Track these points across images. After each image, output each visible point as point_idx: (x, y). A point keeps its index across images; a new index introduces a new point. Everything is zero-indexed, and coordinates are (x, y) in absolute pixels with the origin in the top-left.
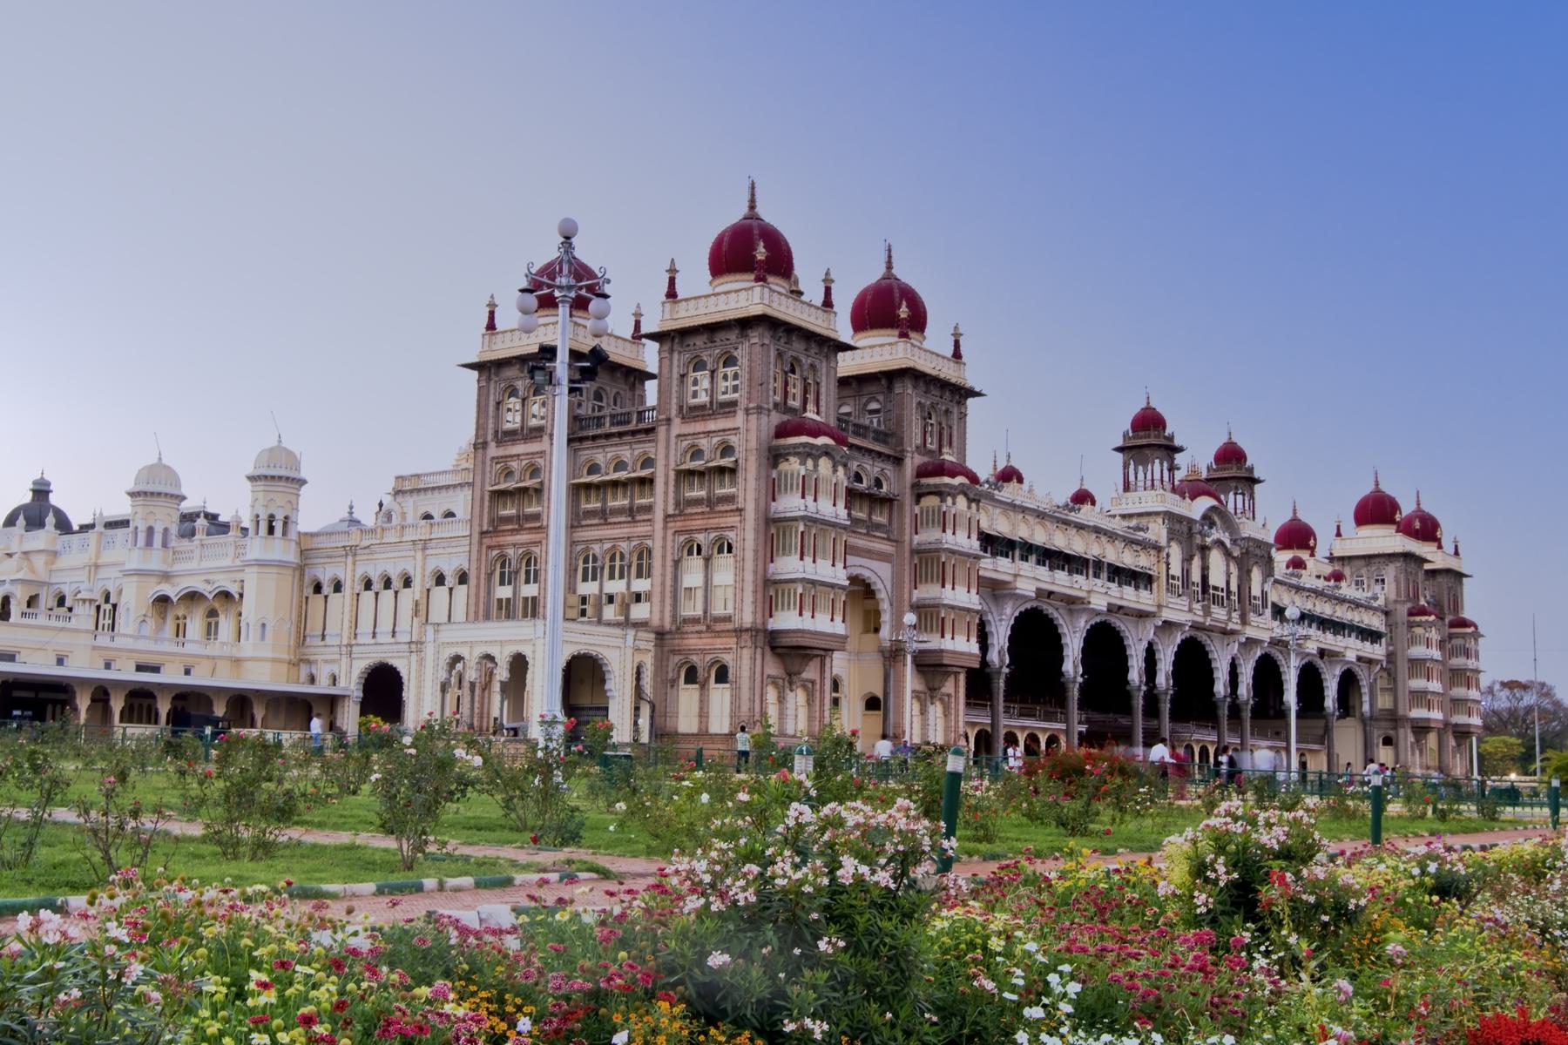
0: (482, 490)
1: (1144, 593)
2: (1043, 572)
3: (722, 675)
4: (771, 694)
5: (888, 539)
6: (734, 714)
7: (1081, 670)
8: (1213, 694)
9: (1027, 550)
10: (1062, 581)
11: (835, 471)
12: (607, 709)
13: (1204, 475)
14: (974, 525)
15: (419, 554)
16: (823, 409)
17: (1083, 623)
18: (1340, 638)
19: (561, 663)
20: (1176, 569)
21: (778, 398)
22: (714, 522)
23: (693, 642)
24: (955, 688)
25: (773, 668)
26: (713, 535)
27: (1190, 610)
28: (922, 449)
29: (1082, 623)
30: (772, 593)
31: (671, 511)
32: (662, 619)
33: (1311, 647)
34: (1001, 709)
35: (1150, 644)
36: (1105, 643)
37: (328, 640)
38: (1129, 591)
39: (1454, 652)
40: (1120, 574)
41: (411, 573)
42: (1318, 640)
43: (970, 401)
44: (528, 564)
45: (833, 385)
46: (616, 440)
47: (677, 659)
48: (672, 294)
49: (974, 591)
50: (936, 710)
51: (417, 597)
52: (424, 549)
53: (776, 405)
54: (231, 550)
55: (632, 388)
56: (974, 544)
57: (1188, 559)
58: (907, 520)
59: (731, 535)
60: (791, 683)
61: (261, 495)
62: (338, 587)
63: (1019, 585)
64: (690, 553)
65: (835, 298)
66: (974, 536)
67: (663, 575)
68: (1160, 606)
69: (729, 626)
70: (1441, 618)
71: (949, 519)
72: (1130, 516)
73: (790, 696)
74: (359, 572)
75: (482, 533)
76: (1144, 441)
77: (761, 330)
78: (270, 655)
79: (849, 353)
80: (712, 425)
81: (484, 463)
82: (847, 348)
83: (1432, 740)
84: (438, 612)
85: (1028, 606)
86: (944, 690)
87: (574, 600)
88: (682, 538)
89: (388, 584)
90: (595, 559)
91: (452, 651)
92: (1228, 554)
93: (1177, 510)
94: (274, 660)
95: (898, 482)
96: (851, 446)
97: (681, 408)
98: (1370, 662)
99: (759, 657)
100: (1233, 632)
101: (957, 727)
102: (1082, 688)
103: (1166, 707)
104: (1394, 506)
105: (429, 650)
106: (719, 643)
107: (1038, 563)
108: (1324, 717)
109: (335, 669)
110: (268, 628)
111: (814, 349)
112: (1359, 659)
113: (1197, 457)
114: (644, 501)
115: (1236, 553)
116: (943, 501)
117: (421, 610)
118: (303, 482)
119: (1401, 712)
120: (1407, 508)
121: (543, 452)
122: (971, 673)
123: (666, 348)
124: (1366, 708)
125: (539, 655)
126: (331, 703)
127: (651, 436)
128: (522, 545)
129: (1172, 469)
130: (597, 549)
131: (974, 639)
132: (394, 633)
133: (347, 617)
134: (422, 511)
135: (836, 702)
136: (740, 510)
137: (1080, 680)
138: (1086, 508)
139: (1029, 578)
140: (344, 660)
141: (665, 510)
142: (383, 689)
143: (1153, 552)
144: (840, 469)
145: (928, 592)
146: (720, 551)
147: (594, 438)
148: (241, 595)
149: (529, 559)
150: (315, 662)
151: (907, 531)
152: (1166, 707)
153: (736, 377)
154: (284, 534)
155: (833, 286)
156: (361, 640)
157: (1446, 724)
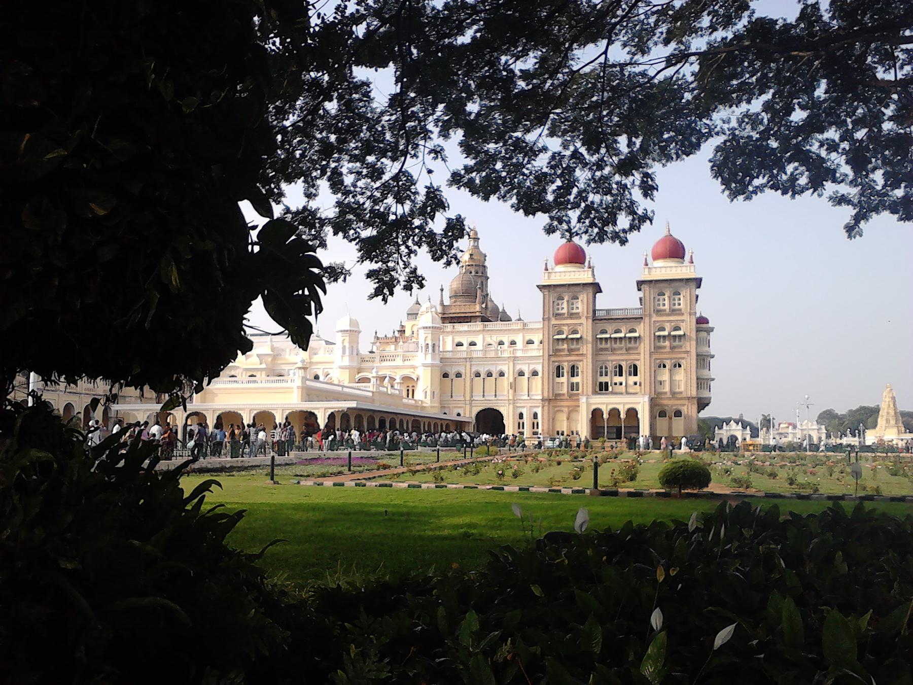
15: (511, 364)
22: (675, 356)
23: (665, 402)
61: (430, 336)
62: (459, 375)
64: (660, 367)
69: (684, 395)
74: (474, 369)
75: (549, 356)
80: (671, 318)
89: (490, 375)
90: (606, 368)
106: (679, 402)
121: (581, 324)
126: (460, 426)
136: (687, 352)
140: (468, 406)
146: (675, 366)
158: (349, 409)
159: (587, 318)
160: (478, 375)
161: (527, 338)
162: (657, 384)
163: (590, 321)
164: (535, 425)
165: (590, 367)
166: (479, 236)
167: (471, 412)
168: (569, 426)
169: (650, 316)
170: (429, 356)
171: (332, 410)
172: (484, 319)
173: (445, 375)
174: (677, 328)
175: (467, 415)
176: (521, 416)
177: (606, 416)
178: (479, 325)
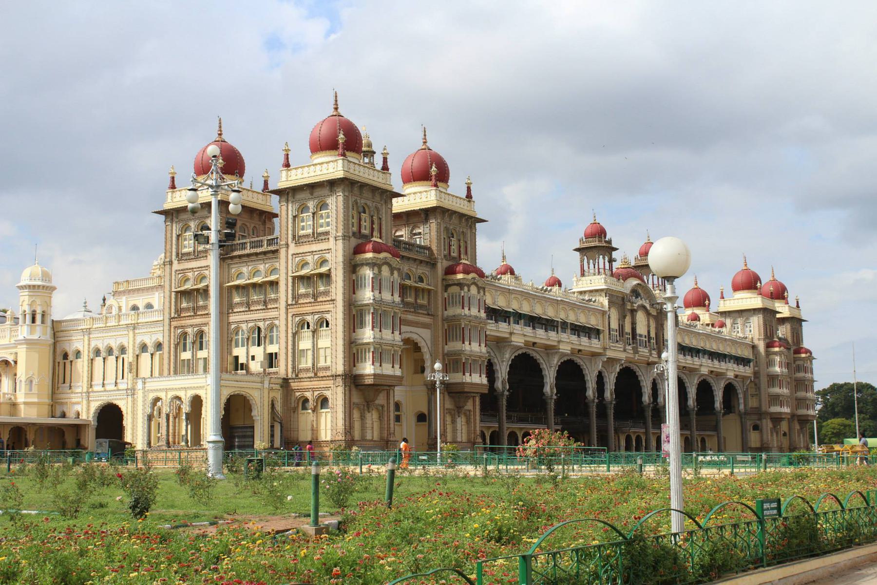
0: (171, 292)
1: (595, 341)
2: (528, 330)
3: (324, 402)
4: (356, 415)
5: (428, 315)
7: (555, 391)
8: (642, 403)
9: (519, 317)
10: (541, 335)
11: (392, 274)
12: (253, 427)
13: (633, 264)
14: (482, 304)
15: (131, 333)
16: (384, 234)
17: (556, 361)
18: (723, 364)
19: (224, 400)
20: (614, 325)
21: (355, 229)
23: (306, 384)
24: (473, 406)
25: (356, 399)
26: (316, 317)
27: (625, 350)
28: (448, 257)
29: (555, 362)
30: (355, 351)
31: (290, 302)
32: (287, 370)
33: (704, 371)
34: (505, 418)
35: (600, 373)
36: (570, 371)
38: (584, 340)
39: (798, 369)
40: (578, 330)
41: (126, 345)
42: (705, 366)
43: (477, 225)
44: (201, 337)
45: (390, 218)
46: (254, 258)
48: (287, 165)
49: (483, 345)
50: (461, 421)
51: (131, 360)
52: (134, 328)
53: (354, 234)
54: (8, 333)
55: (264, 223)
56: (483, 315)
57: (622, 317)
58: (440, 302)
59: (328, 316)
60: (368, 408)
62: (78, 354)
63: (514, 338)
64: (302, 328)
65: (390, 164)
66: (482, 311)
67: (287, 343)
68: (605, 349)
69: (329, 373)
70: (789, 349)
71: (466, 299)
72: (585, 292)
73: (368, 415)
74: (93, 344)
75: (171, 319)
76: (593, 244)
77: (342, 187)
78: (36, 400)
79: (400, 199)
80: (315, 247)
81: (171, 274)
82: (398, 195)
83: (784, 426)
84: (145, 371)
85: (520, 352)
86: (466, 408)
87: (230, 359)
88: (297, 319)
89: (110, 351)
92: (648, 314)
93: (614, 288)
95: (433, 280)
96: (403, 257)
97: (294, 237)
98: (744, 378)
99: (347, 392)
100: (655, 363)
101: (475, 430)
102: (557, 402)
103: (611, 412)
104: (757, 279)
105: (140, 395)
106: (322, 384)
107: (525, 325)
108: (715, 414)
110: (34, 383)
111: (378, 198)
112: (736, 376)
113: (626, 252)
115: (655, 313)
116: (462, 289)
117: (135, 369)
118: (53, 289)
119: (764, 409)
120: (765, 278)
122: (483, 396)
123: (283, 199)
124: (742, 407)
125: (209, 396)
126: (78, 429)
128: (197, 325)
129: (611, 261)
130: (244, 326)
131: (484, 376)
132: (116, 383)
134: (131, 304)
135: (398, 419)
137: (555, 397)
138: (556, 288)
139: (521, 336)
140: (85, 402)
141: (287, 302)
142: (110, 418)
143: (599, 316)
144: (396, 273)
145: (455, 346)
146: (321, 326)
147: (240, 257)
148: (16, 362)
149: (201, 334)
151: (440, 309)
152: (611, 412)
154: (43, 322)
155: (388, 157)
156: (95, 388)
157: (793, 415)
160: (97, 352)
167: (88, 410)
169: (287, 245)
175: (84, 416)
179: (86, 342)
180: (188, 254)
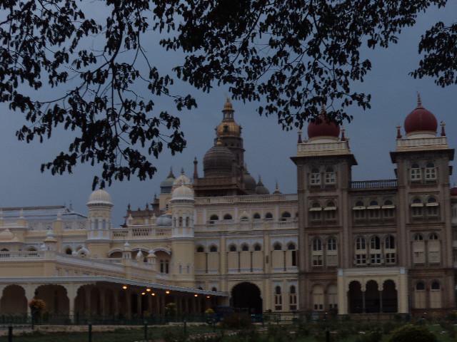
6: (443, 301)
15: (267, 237)
22: (430, 227)
23: (423, 274)
31: (408, 222)
37: (209, 273)
47: (415, 280)
51: (267, 254)
59: (438, 233)
62: (213, 249)
64: (416, 239)
67: (406, 248)
74: (229, 243)
80: (425, 190)
89: (245, 248)
90: (363, 240)
91: (353, 279)
94: (193, 282)
106: (437, 274)
109: (216, 286)
114: (389, 217)
121: (337, 196)
126: (216, 300)
127: (394, 192)
133: (223, 263)
136: (444, 223)
142: (247, 295)
146: (431, 238)
150: (204, 282)
153: (433, 171)
158: (98, 283)
159: (342, 190)
160: (233, 248)
161: (283, 211)
162: (415, 255)
163: (345, 193)
164: (292, 299)
165: (346, 240)
166: (234, 108)
168: (326, 300)
169: (404, 187)
170: (184, 230)
171: (82, 285)
172: (240, 192)
173: (200, 249)
174: (432, 200)
176: (278, 290)
177: (363, 289)
178: (236, 199)
179: (223, 241)
180: (318, 186)
